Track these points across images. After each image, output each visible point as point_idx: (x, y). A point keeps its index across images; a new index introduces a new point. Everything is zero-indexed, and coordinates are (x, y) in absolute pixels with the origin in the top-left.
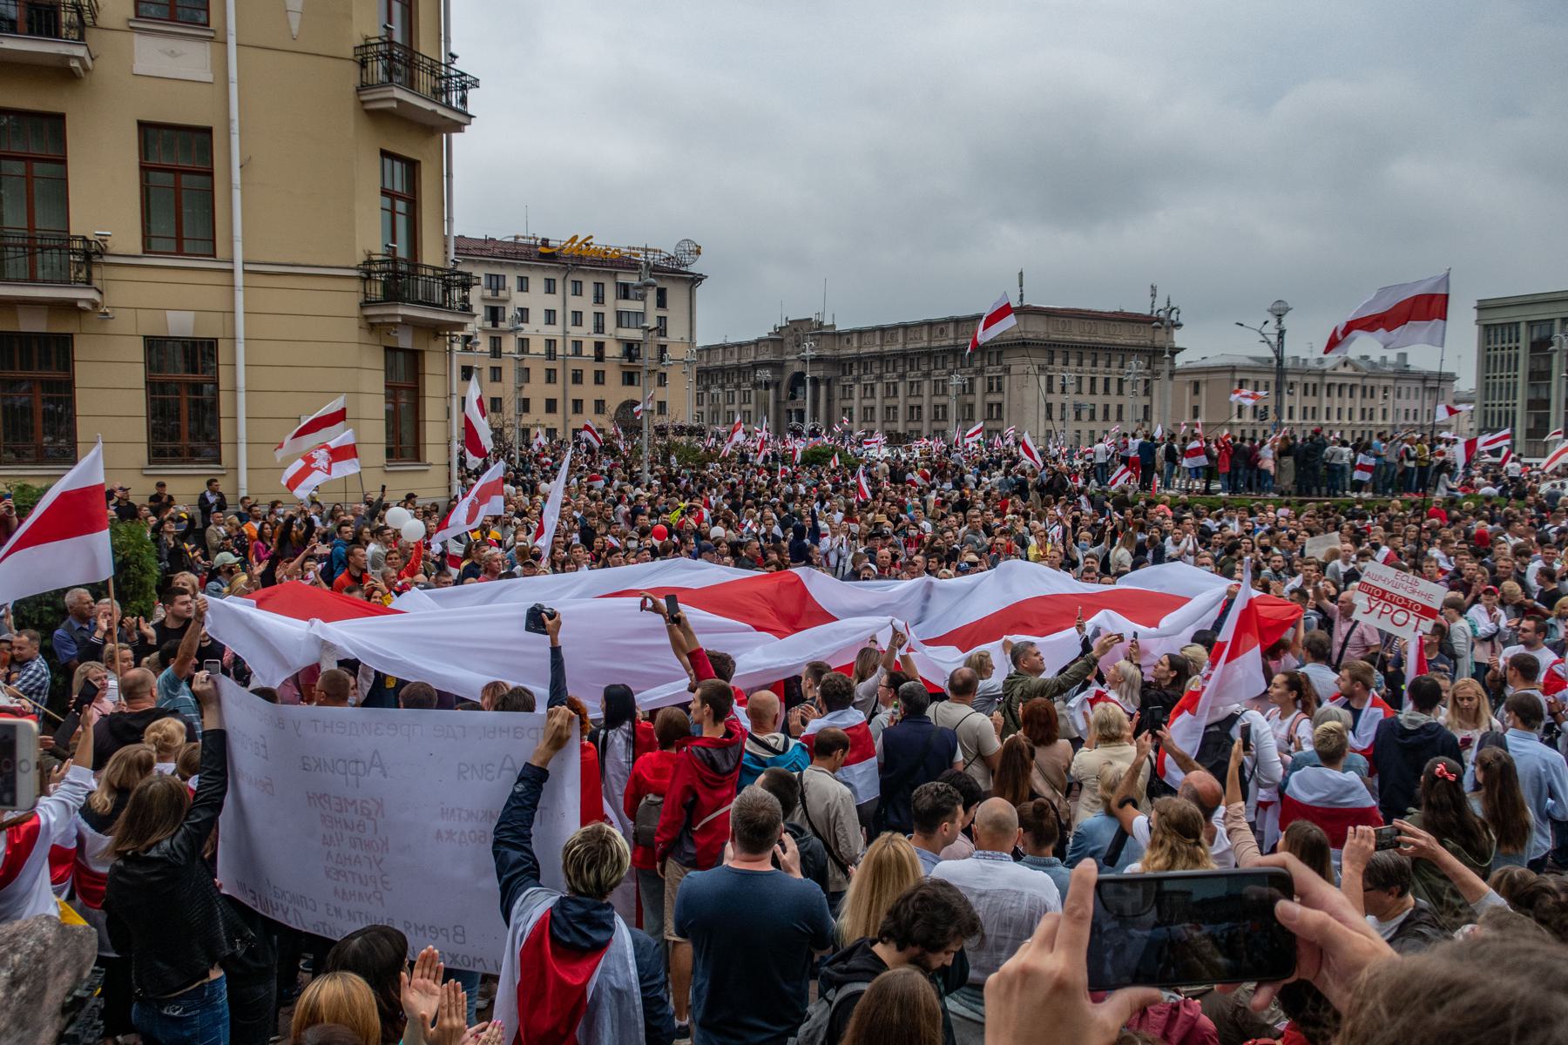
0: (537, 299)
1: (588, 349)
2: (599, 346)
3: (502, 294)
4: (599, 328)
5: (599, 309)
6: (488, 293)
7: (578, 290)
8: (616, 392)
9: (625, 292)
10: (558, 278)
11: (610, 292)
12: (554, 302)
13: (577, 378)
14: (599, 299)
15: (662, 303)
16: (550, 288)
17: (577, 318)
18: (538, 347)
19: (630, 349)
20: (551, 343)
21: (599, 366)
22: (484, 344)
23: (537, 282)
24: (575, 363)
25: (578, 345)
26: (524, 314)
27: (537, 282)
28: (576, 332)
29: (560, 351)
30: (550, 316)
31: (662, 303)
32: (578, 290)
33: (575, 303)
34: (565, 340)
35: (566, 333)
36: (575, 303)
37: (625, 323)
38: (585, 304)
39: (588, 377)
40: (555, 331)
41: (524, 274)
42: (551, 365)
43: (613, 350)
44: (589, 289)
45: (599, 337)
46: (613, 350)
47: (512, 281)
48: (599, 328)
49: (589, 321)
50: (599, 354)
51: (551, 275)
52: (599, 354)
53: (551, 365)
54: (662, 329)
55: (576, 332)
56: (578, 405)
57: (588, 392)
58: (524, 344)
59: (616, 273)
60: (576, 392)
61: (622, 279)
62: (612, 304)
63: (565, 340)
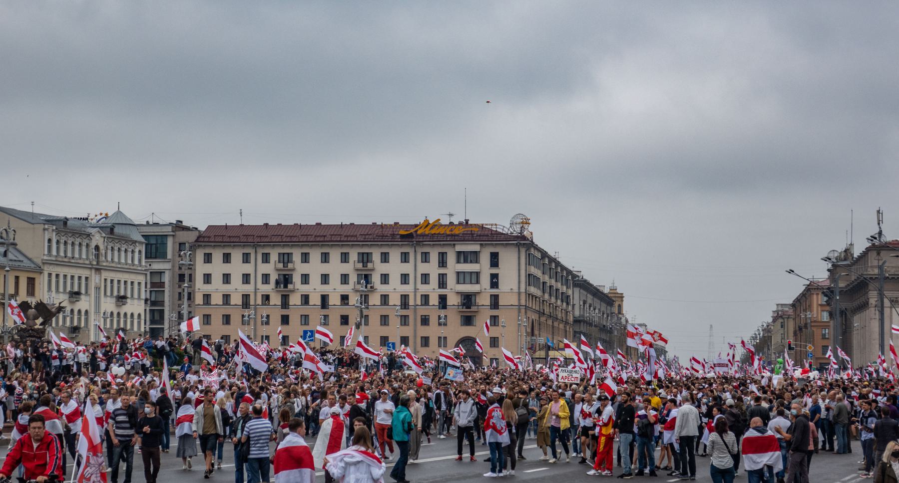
0: (395, 267)
1: (434, 300)
2: (443, 299)
3: (370, 265)
4: (442, 283)
5: (442, 271)
6: (360, 266)
7: (426, 258)
8: (456, 331)
10: (411, 251)
11: (451, 258)
12: (407, 268)
13: (425, 321)
14: (443, 263)
16: (405, 258)
17: (425, 278)
18: (395, 300)
19: (468, 300)
20: (405, 298)
22: (354, 299)
24: (423, 311)
25: (426, 298)
27: (395, 255)
28: (423, 289)
29: (411, 302)
32: (426, 258)
33: (423, 268)
34: (415, 295)
35: (416, 289)
36: (423, 268)
37: (461, 280)
38: (432, 268)
39: (433, 320)
40: (408, 289)
41: (385, 250)
42: (404, 312)
43: (453, 300)
44: (434, 257)
45: (443, 291)
46: (453, 300)
47: (376, 257)
48: (442, 283)
53: (404, 312)
55: (423, 289)
56: (425, 341)
57: (433, 331)
58: (385, 299)
59: (454, 245)
60: (423, 331)
61: (460, 248)
62: (453, 267)
63: (415, 295)
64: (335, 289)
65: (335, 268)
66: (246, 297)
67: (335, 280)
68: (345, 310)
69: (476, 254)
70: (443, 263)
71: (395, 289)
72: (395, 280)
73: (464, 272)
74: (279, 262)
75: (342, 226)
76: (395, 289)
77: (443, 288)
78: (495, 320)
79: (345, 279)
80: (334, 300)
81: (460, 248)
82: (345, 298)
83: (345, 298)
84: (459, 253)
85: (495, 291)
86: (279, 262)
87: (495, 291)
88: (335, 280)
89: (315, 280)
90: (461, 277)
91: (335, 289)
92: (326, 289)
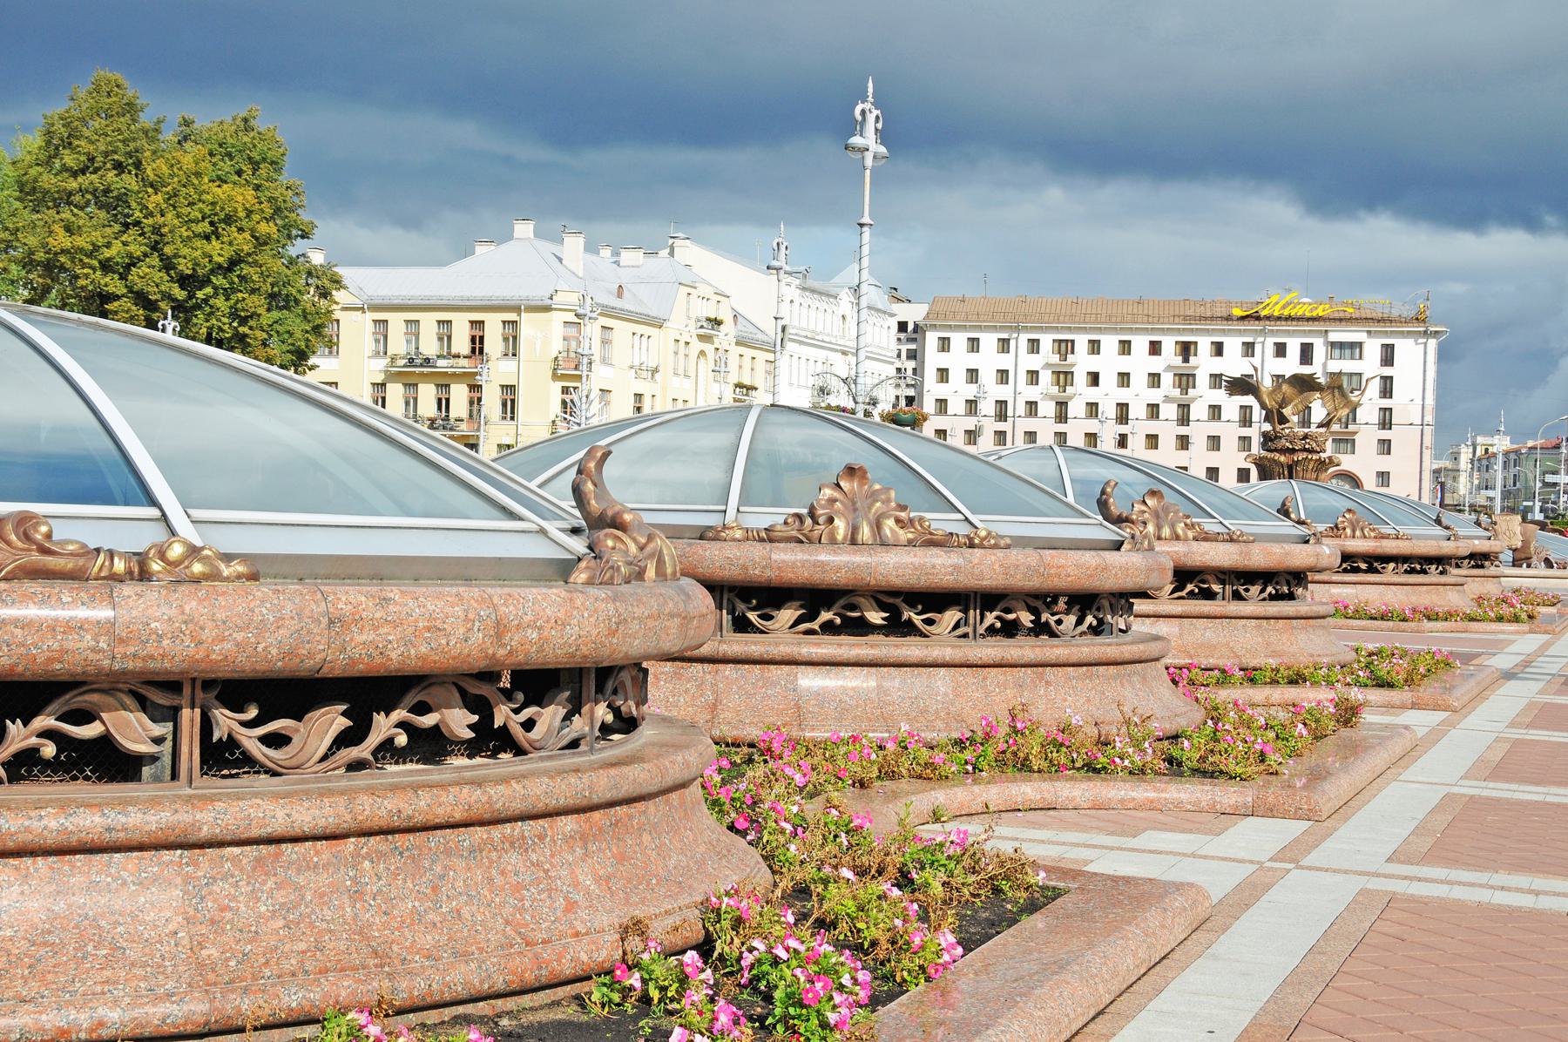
15: (1388, 357)
31: (1388, 357)
61: (1339, 335)
64: (1139, 396)
65: (1140, 363)
66: (1002, 404)
67: (1139, 380)
68: (1153, 427)
69: (1360, 345)
78: (1385, 446)
79: (1155, 380)
80: (1137, 411)
81: (1339, 335)
84: (1333, 345)
85: (1386, 403)
87: (1386, 403)
88: (1139, 380)
91: (1139, 396)
92: (1123, 395)
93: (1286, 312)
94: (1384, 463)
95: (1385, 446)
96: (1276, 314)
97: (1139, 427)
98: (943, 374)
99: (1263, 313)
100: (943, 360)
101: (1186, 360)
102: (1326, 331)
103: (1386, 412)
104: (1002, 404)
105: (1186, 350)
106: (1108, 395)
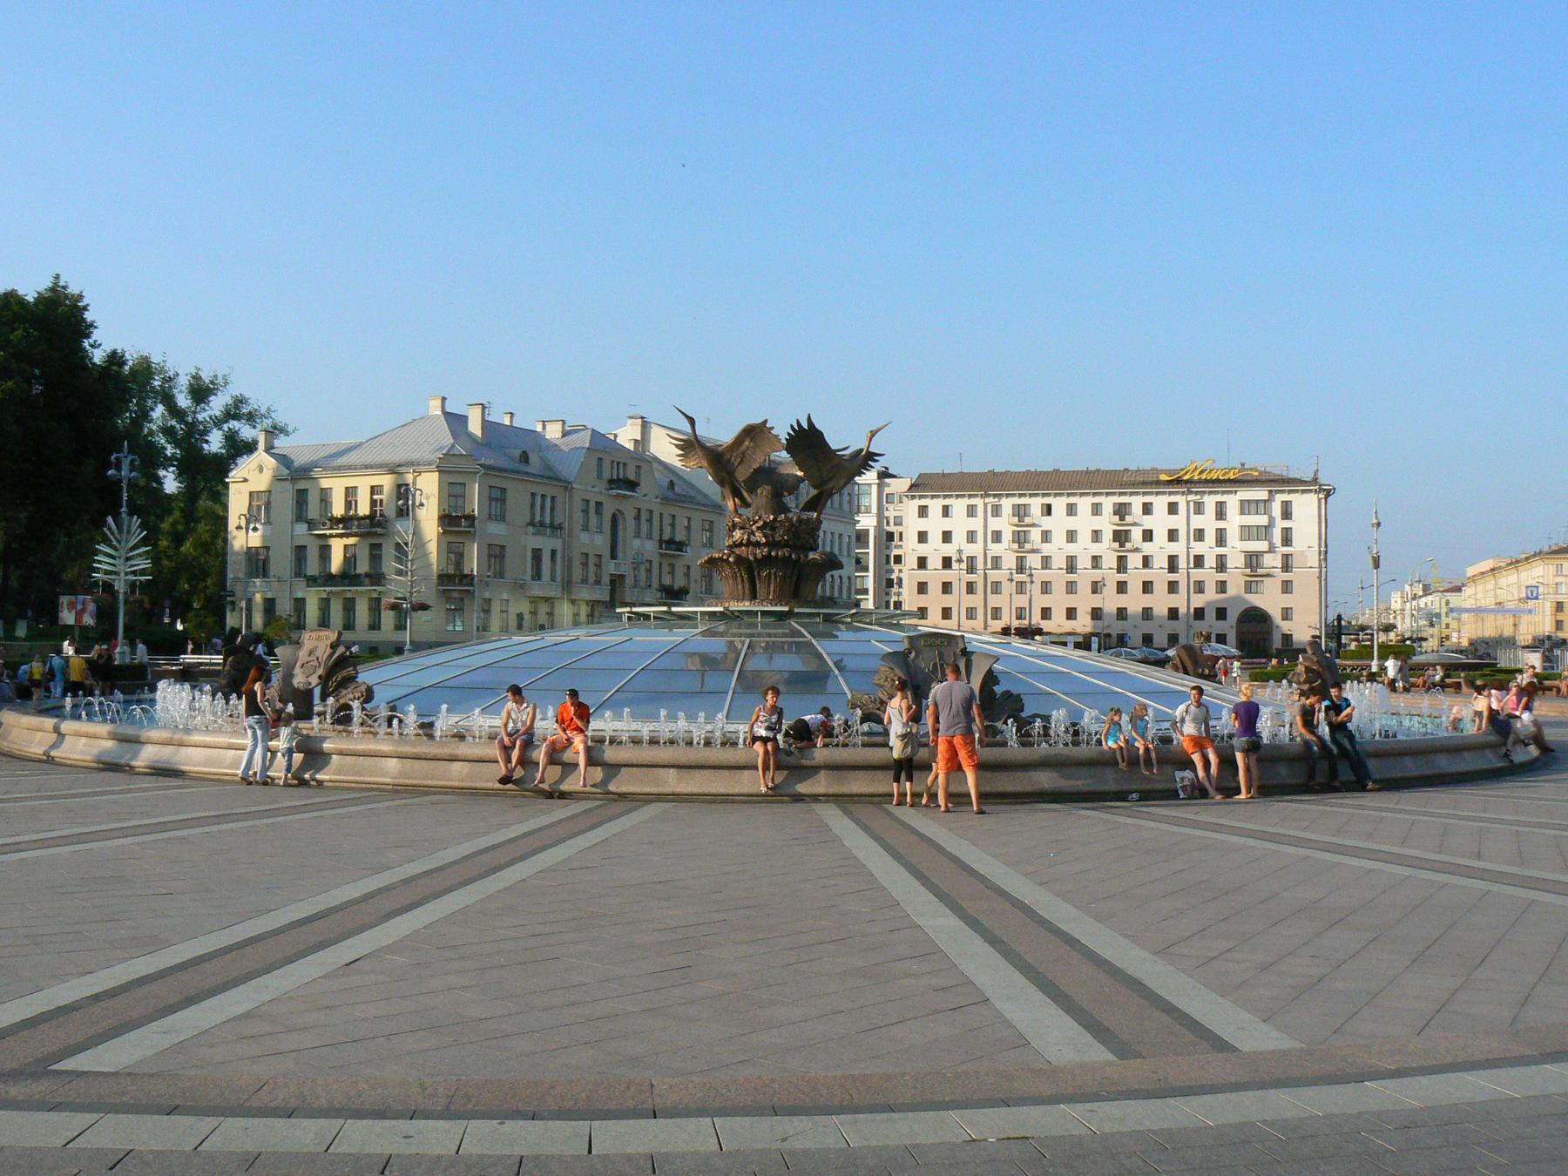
1: (1210, 561)
4: (1221, 539)
5: (1221, 524)
9: (1245, 506)
14: (1221, 514)
16: (1173, 509)
18: (1161, 562)
19: (1253, 560)
21: (1222, 577)
22: (1110, 561)
23: (1160, 503)
26: (1148, 535)
30: (1173, 535)
36: (1197, 522)
38: (1208, 522)
42: (1173, 577)
46: (1236, 561)
47: (1137, 508)
48: (1221, 539)
49: (1210, 537)
50: (1221, 565)
51: (1173, 499)
52: (1221, 565)
53: (1173, 577)
54: (1287, 539)
58: (1146, 562)
64: (1084, 549)
65: (1084, 522)
67: (1084, 537)
70: (1221, 514)
71: (1160, 549)
72: (1160, 536)
73: (1249, 526)
74: (1014, 515)
75: (1088, 472)
76: (1160, 549)
77: (1221, 546)
79: (1096, 536)
80: (1084, 562)
82: (1096, 561)
83: (1096, 561)
86: (1014, 515)
88: (1084, 537)
89: (1059, 538)
90: (1247, 532)
91: (1084, 549)
92: (1072, 549)
93: (1204, 477)
94: (1287, 600)
95: (1287, 587)
96: (1196, 478)
97: (1085, 576)
98: (923, 537)
99: (1185, 478)
100: (922, 524)
101: (1122, 518)
102: (1236, 491)
103: (1286, 558)
104: (972, 559)
105: (1121, 511)
106: (1058, 549)
